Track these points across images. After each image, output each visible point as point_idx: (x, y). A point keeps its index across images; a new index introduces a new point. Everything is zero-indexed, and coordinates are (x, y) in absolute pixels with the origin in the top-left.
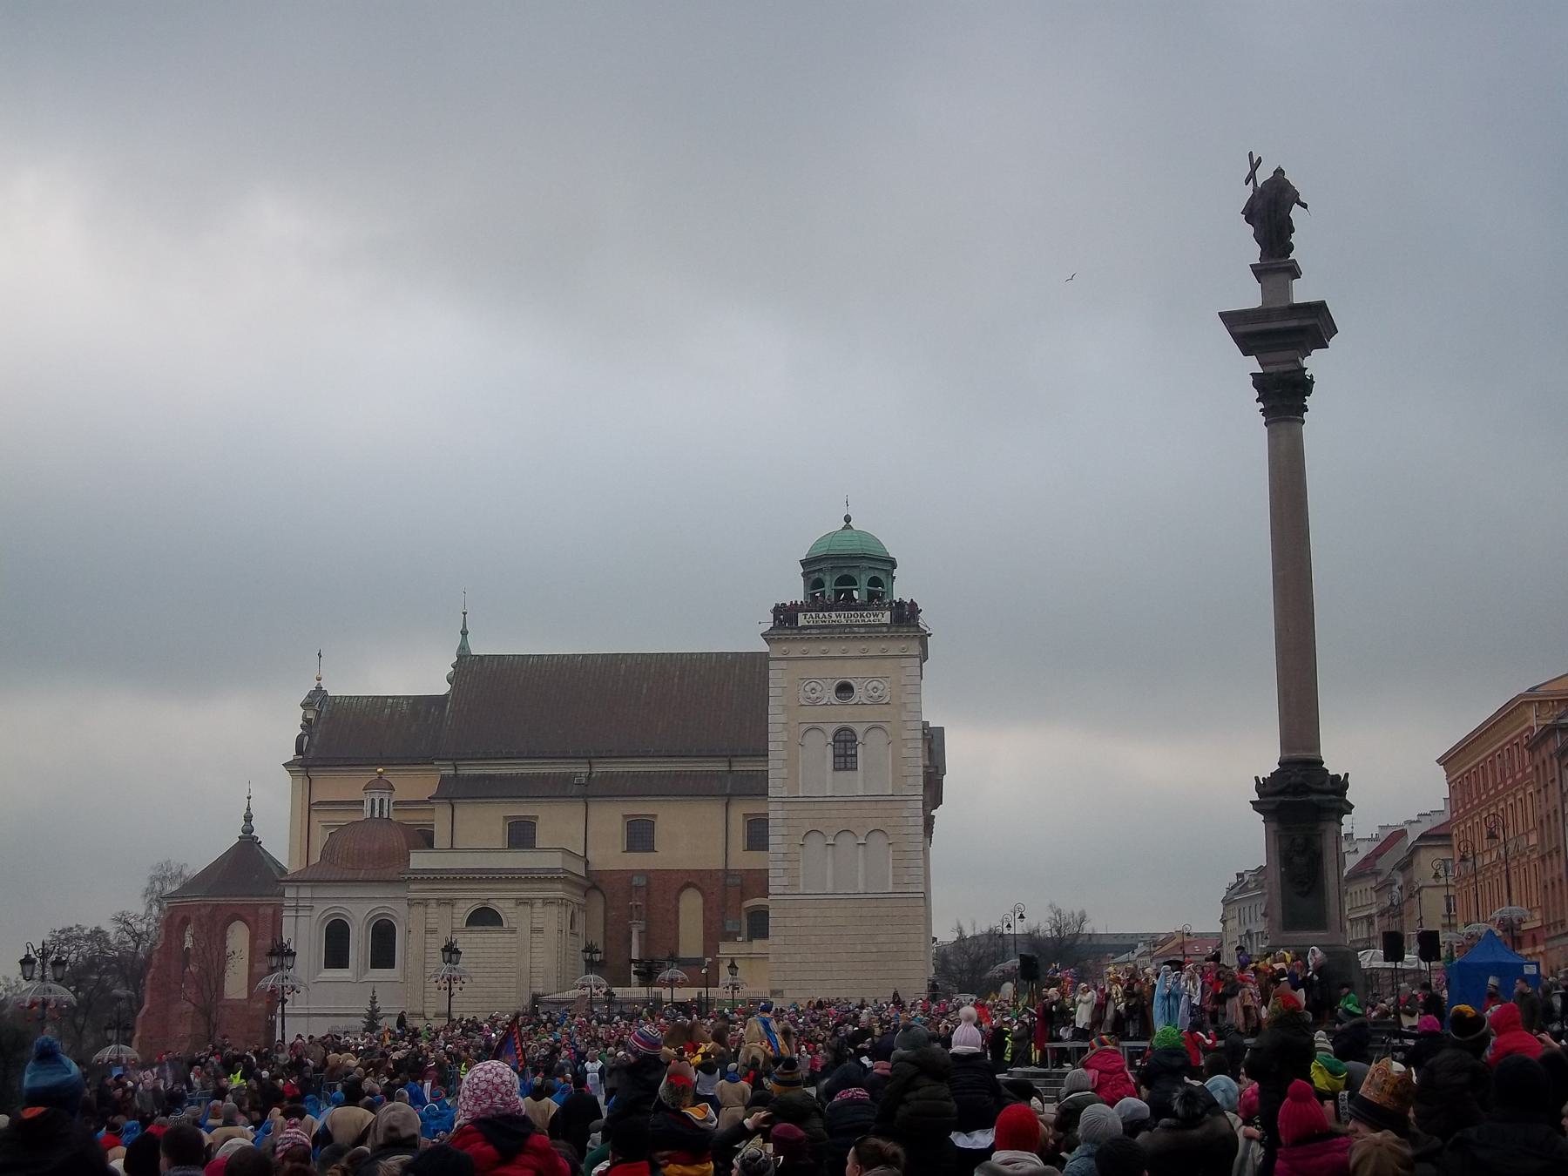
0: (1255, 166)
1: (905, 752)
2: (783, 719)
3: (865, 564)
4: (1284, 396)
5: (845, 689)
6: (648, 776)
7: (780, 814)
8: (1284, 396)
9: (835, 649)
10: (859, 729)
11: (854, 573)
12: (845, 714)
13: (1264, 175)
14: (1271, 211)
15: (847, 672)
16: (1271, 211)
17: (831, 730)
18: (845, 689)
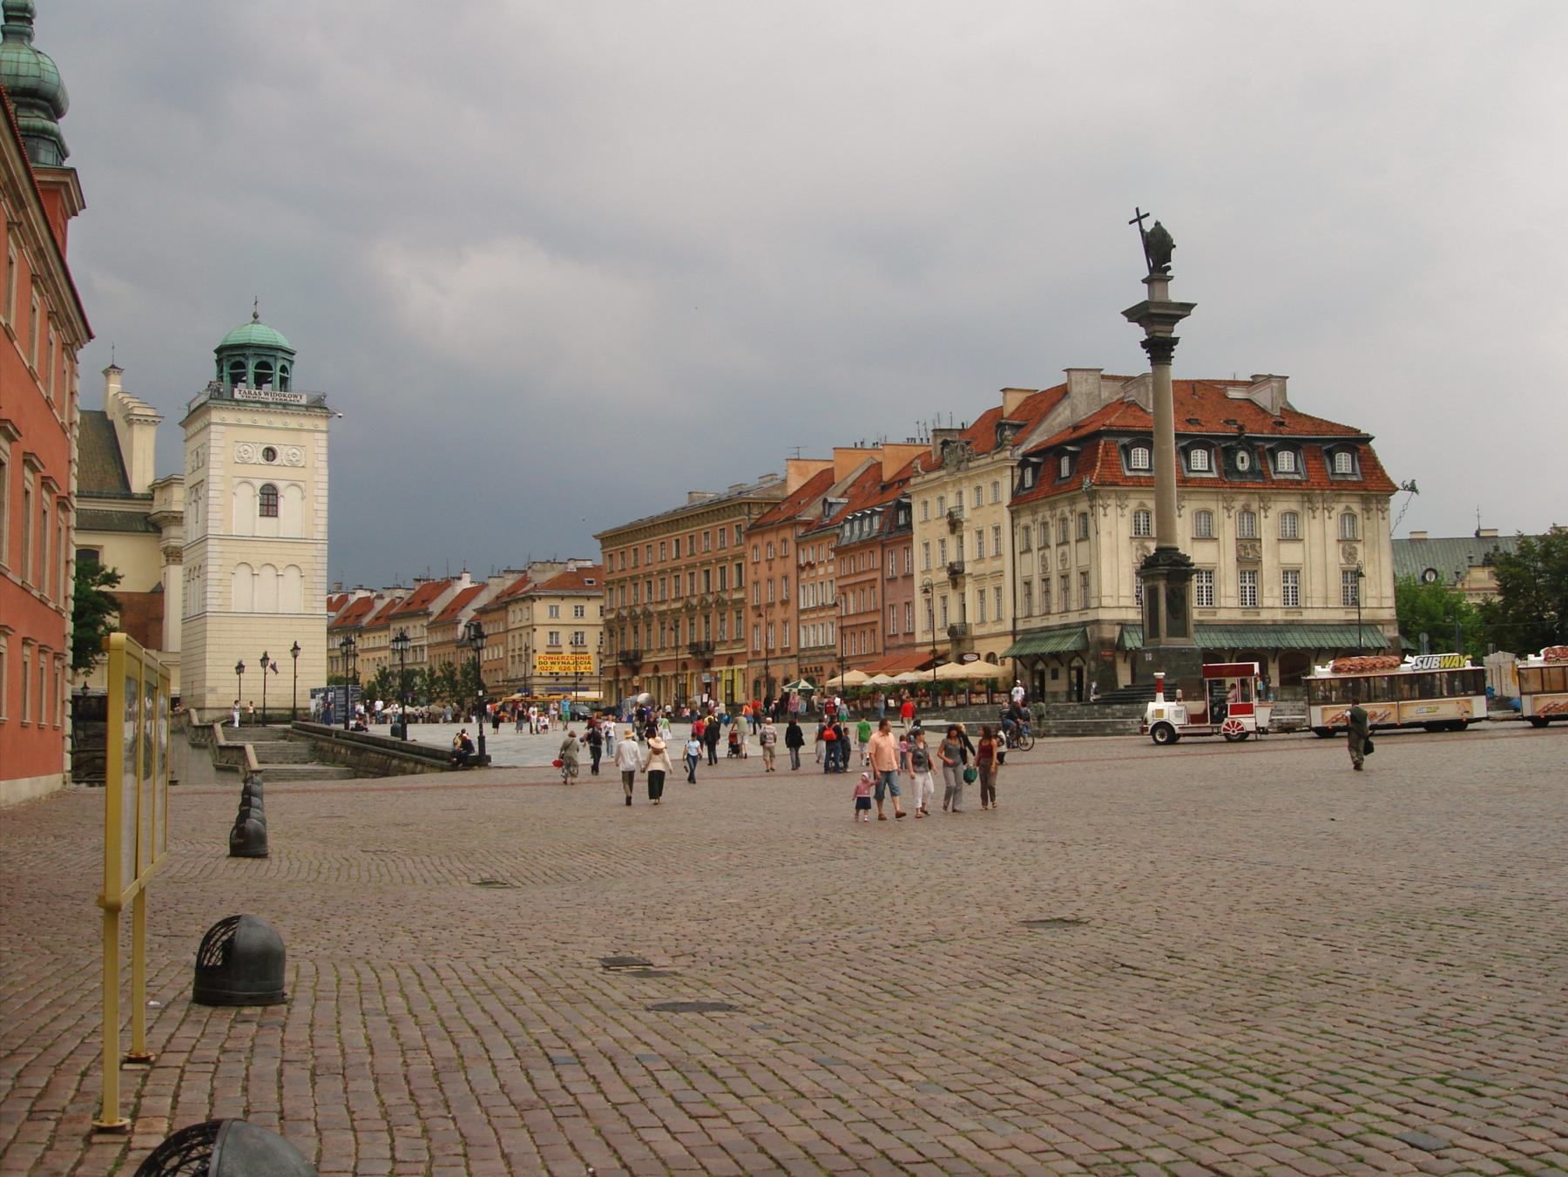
0: (1139, 219)
1: (316, 506)
2: (222, 472)
3: (280, 354)
4: (1160, 349)
5: (270, 454)
6: (108, 514)
7: (218, 549)
8: (1160, 349)
9: (262, 420)
10: (281, 485)
11: (271, 361)
12: (269, 473)
13: (1148, 225)
14: (1158, 247)
15: (272, 439)
16: (1158, 247)
17: (259, 484)
18: (270, 454)
